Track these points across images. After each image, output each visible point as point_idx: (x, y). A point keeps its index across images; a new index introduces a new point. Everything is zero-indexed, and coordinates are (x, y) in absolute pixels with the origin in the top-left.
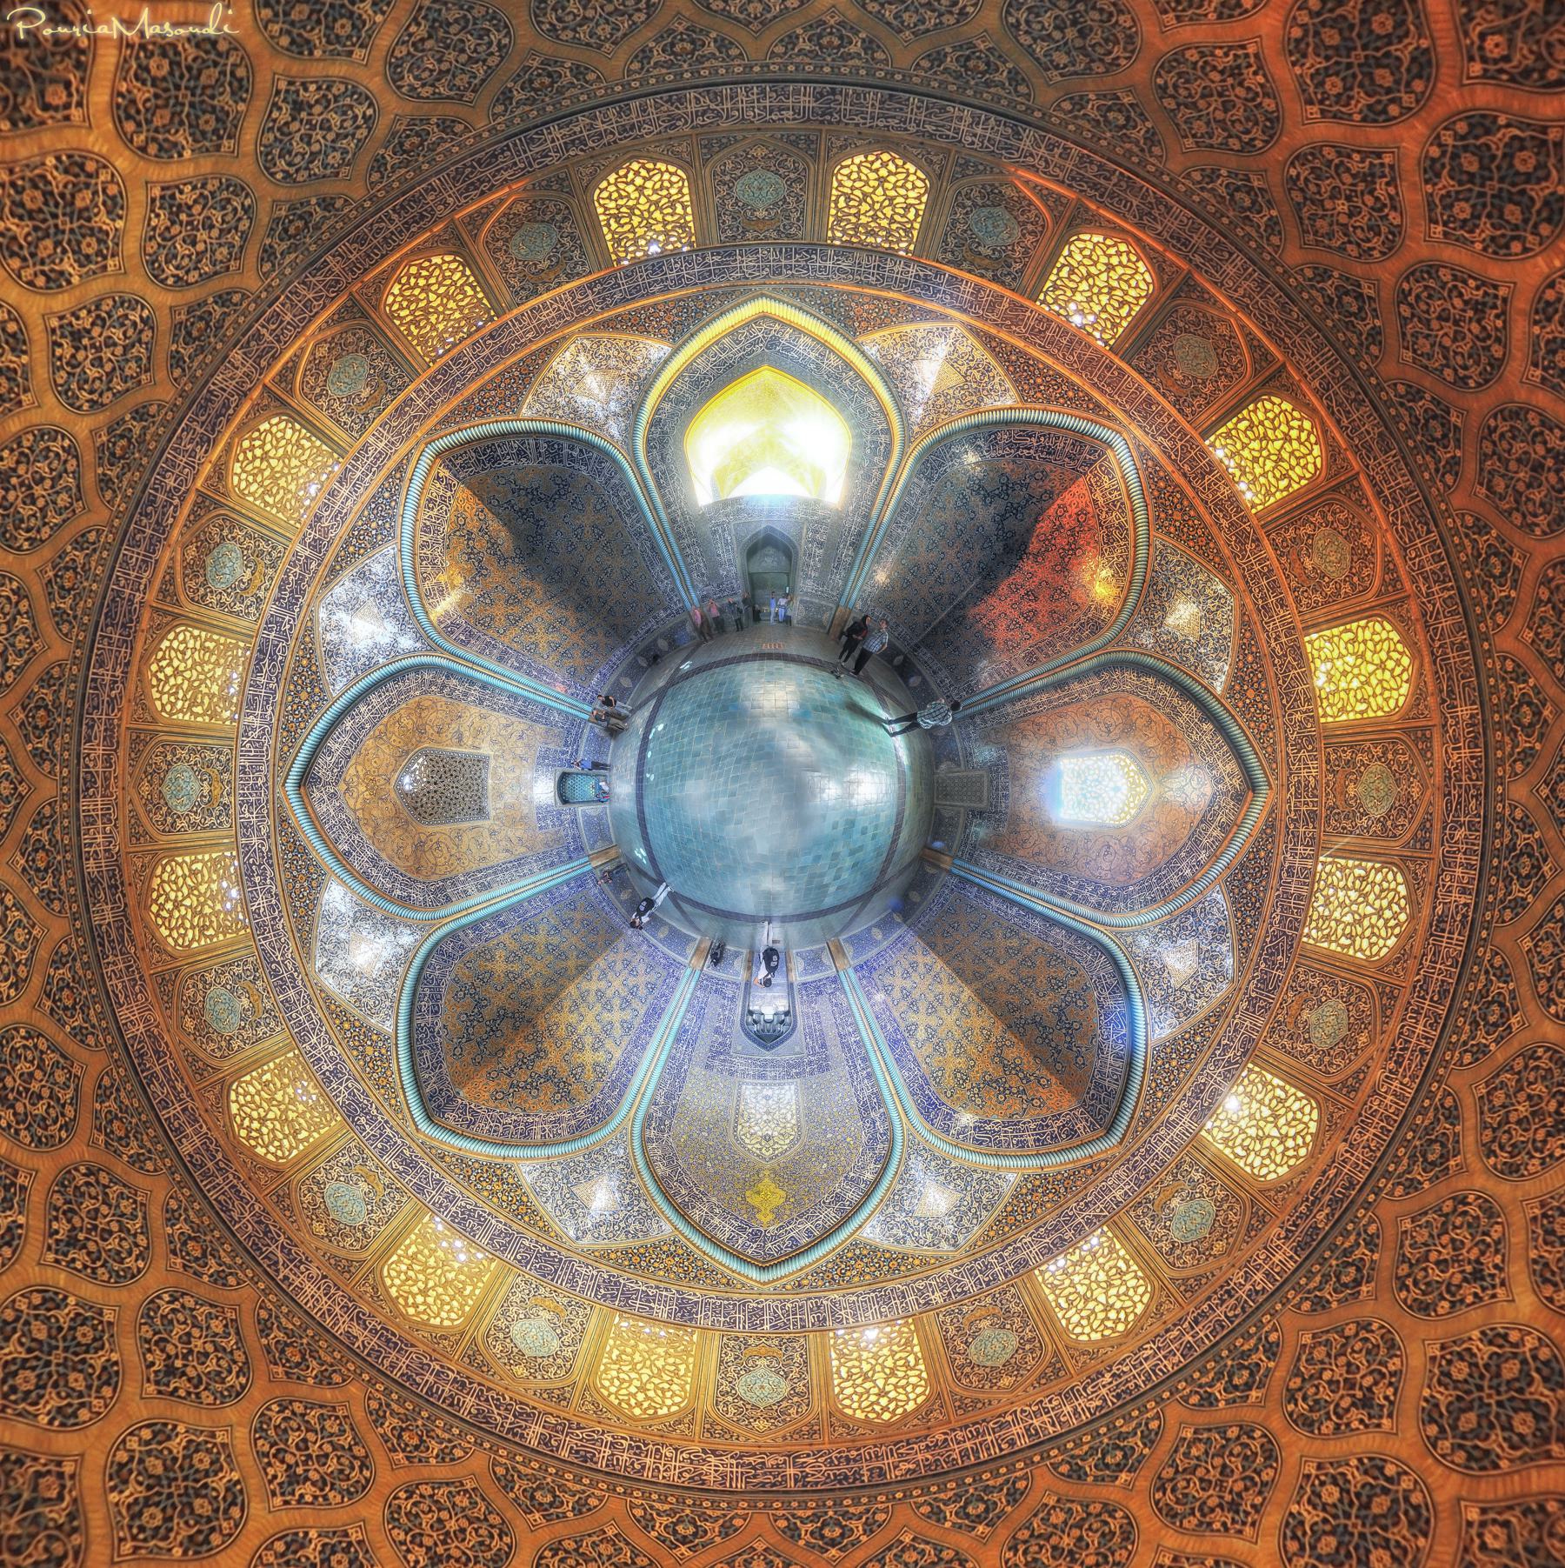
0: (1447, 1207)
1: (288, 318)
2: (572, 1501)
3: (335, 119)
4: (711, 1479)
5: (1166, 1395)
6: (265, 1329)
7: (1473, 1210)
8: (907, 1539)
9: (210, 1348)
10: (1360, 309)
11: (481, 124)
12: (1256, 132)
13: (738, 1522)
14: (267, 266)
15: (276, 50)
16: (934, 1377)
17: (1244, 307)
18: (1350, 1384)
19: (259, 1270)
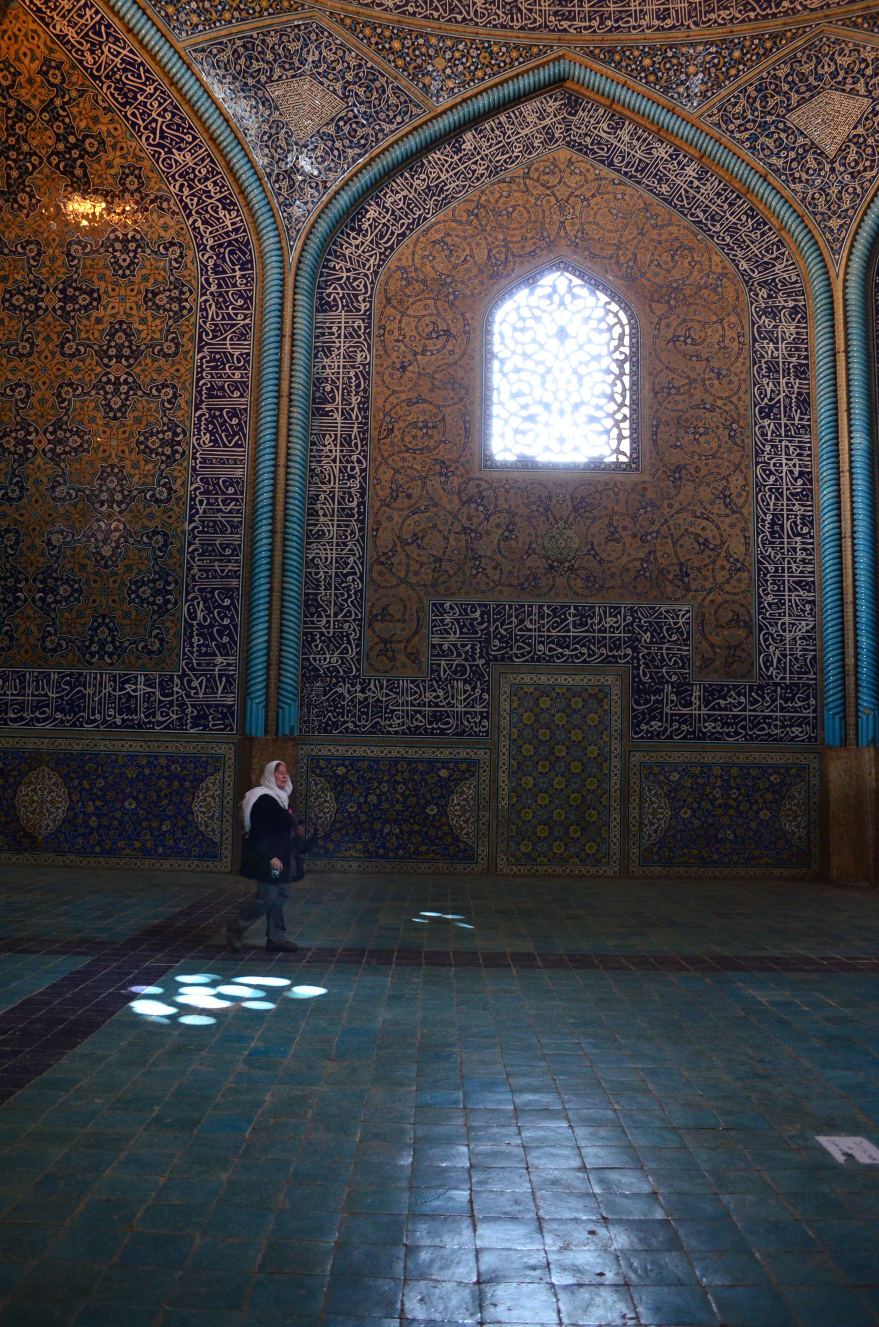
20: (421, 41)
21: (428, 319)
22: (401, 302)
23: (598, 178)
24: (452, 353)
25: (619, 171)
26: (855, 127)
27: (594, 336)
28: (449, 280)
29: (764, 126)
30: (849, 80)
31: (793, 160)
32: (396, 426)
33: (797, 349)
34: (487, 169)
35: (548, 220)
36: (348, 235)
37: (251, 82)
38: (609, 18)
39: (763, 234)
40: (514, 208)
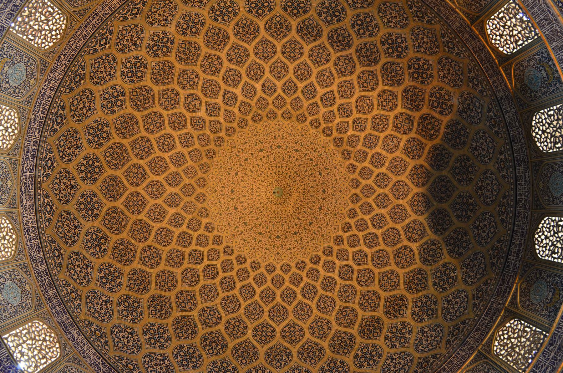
1: (455, 363)
2: (53, 245)
3: (458, 300)
4: (32, 202)
5: (83, 54)
6: (106, 343)
7: (172, 6)
8: (57, 142)
9: (122, 339)
10: (417, 13)
11: (493, 276)
12: (444, 61)
13: (45, 193)
14: (448, 346)
15: (440, 293)
16: (11, 105)
17: (453, 10)
19: (108, 361)
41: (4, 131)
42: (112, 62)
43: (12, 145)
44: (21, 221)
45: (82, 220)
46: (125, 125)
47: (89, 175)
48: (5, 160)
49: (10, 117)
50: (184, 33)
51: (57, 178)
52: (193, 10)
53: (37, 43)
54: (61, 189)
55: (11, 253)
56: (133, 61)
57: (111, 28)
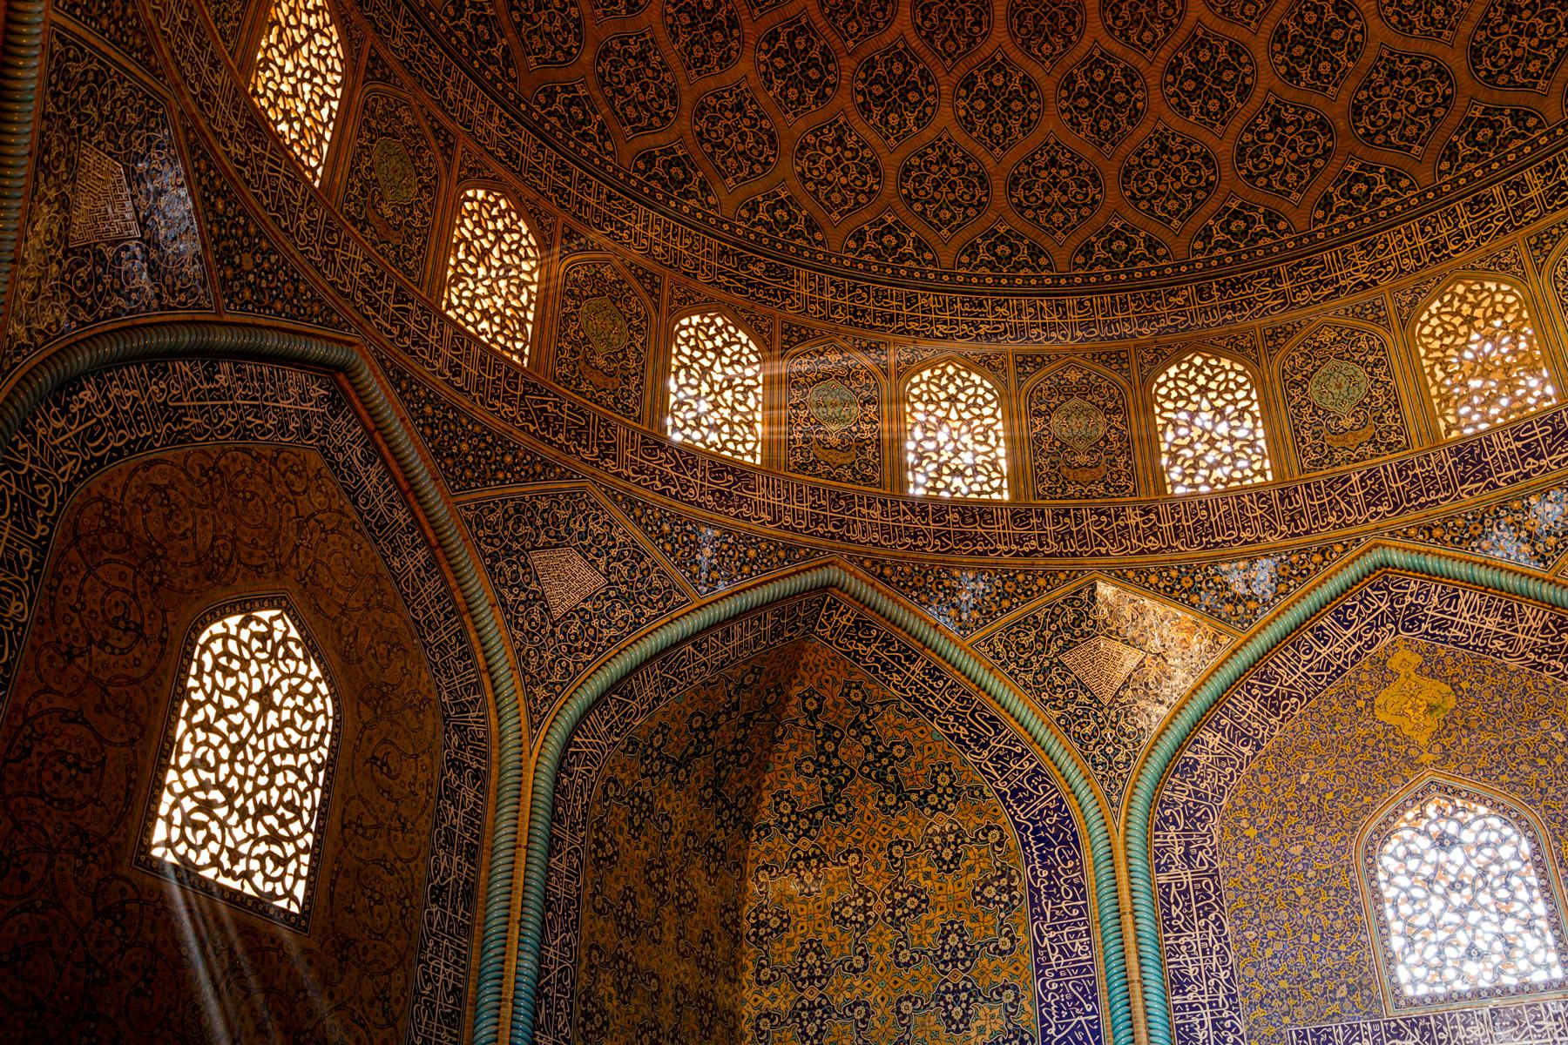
0: (707, 147)
7: (704, 124)
13: (1320, 214)
18: (838, 160)
20: (242, 221)
21: (119, 596)
22: (92, 550)
23: (341, 512)
24: (137, 663)
25: (361, 515)
26: (585, 601)
27: (298, 718)
28: (159, 552)
29: (508, 549)
30: (594, 551)
31: (522, 602)
32: (37, 748)
33: (472, 824)
34: (235, 423)
35: (283, 534)
36: (48, 408)
37: (74, 124)
38: (408, 335)
39: (466, 668)
40: (254, 494)
41: (1212, 395)
42: (914, 174)
43: (1233, 361)
44: (1415, 276)
45: (1368, 57)
46: (1045, 22)
47: (1228, 76)
48: (1275, 369)
49: (1174, 394)
50: (734, 23)
51: (1269, 185)
52: (672, 52)
53: (993, 416)
54: (1294, 157)
55: (1506, 293)
56: (877, 112)
57: (852, 244)
